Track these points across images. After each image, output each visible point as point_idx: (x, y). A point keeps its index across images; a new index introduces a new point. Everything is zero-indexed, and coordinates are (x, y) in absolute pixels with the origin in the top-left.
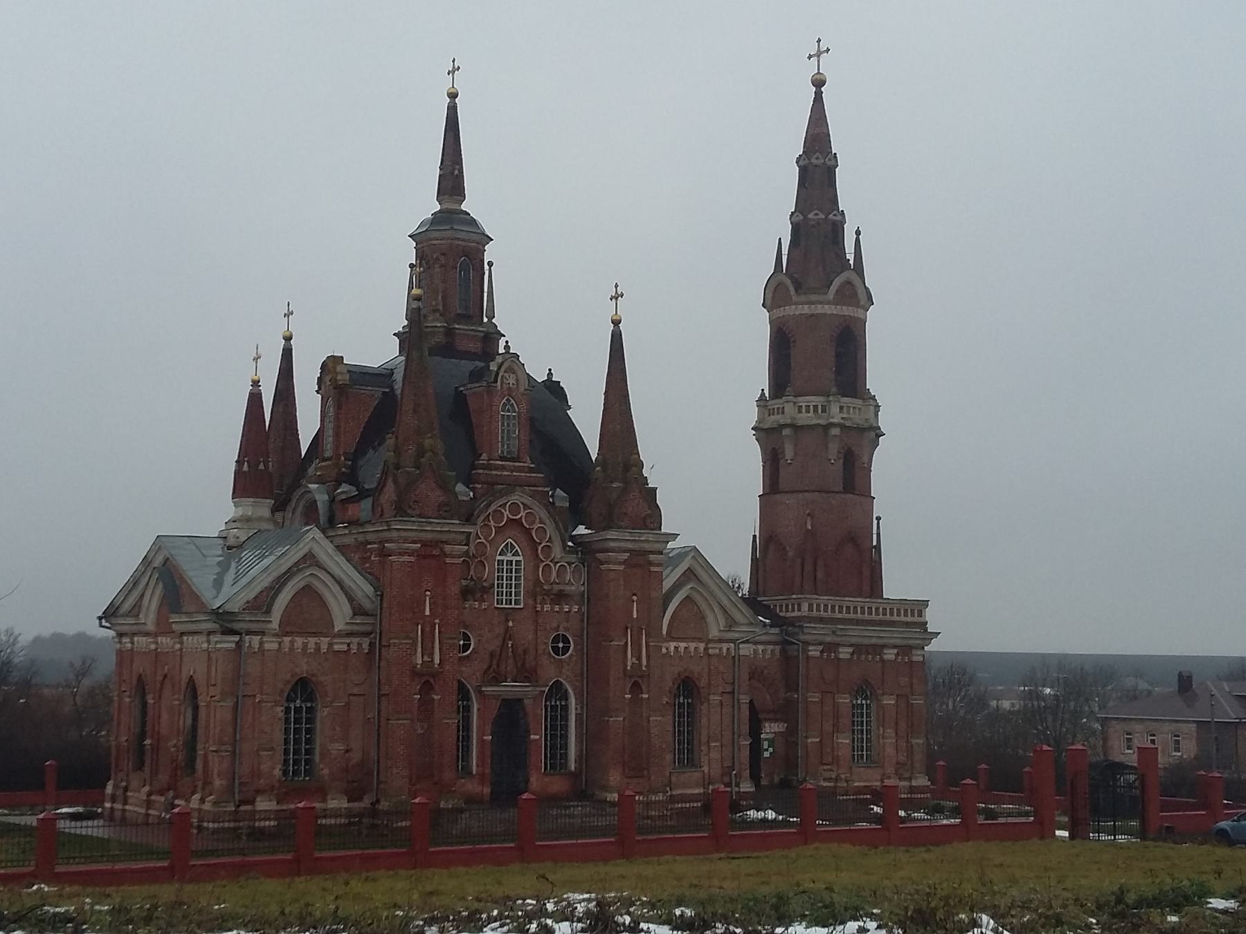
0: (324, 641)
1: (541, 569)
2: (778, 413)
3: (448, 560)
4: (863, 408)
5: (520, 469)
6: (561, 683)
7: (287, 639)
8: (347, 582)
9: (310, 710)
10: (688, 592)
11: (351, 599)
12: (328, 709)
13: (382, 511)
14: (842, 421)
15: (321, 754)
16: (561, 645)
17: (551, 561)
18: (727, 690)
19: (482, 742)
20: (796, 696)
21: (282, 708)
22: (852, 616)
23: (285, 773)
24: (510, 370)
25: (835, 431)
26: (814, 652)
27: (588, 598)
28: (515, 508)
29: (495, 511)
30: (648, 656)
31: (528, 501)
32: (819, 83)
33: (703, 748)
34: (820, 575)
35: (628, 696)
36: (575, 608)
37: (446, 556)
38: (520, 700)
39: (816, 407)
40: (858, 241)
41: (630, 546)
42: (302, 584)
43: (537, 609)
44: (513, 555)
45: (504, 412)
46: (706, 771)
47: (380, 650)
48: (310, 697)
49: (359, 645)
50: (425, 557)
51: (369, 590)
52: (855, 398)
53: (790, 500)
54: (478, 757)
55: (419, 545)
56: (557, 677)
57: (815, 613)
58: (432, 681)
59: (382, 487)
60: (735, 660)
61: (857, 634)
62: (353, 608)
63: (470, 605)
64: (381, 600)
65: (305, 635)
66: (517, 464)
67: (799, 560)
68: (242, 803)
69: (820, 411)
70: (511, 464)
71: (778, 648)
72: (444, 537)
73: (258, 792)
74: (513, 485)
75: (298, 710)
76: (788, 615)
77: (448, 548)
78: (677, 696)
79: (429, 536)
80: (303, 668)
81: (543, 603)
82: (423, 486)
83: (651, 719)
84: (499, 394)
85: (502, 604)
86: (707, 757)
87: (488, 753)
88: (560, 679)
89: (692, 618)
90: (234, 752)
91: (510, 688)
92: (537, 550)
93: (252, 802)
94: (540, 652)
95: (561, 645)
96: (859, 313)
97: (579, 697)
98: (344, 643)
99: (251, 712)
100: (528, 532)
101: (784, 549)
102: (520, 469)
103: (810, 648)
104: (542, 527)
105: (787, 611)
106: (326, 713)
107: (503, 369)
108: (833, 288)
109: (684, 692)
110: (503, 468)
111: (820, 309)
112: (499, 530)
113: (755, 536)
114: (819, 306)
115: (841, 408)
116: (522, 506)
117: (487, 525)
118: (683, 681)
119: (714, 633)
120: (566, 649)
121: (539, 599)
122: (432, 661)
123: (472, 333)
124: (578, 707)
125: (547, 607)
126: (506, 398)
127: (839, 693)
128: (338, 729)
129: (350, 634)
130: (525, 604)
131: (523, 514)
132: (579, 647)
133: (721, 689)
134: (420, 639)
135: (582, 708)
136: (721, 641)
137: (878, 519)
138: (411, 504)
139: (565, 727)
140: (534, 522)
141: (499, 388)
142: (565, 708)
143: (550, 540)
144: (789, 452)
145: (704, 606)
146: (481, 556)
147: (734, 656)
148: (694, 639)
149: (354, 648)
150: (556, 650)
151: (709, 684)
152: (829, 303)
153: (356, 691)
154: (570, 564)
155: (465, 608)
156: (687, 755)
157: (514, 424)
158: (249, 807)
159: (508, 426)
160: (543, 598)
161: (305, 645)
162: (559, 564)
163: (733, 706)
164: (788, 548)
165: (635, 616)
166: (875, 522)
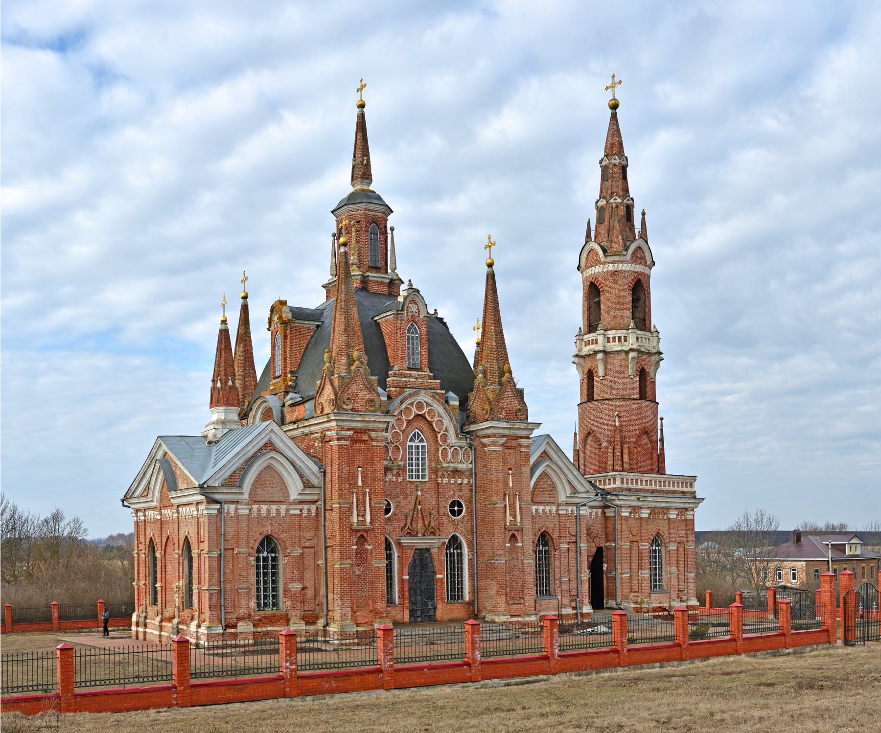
0: (283, 507)
1: (440, 452)
2: (592, 344)
3: (374, 444)
4: (651, 339)
6: (457, 536)
7: (255, 507)
8: (298, 463)
9: (274, 559)
10: (545, 469)
11: (301, 476)
12: (287, 558)
13: (323, 408)
14: (639, 347)
15: (285, 591)
16: (456, 508)
17: (447, 446)
18: (572, 541)
19: (402, 581)
20: (614, 545)
21: (253, 558)
22: (649, 487)
23: (259, 605)
24: (413, 301)
26: (625, 513)
27: (475, 473)
28: (420, 406)
29: (406, 408)
30: (521, 515)
31: (429, 400)
33: (557, 582)
34: (626, 458)
35: (508, 545)
36: (466, 481)
37: (373, 440)
38: (428, 550)
39: (620, 338)
40: (643, 220)
41: (506, 432)
43: (439, 482)
44: (419, 442)
45: (409, 333)
46: (560, 599)
47: (325, 513)
48: (273, 550)
49: (309, 510)
50: (356, 441)
51: (315, 468)
52: (645, 330)
53: (603, 406)
54: (399, 592)
55: (353, 432)
56: (454, 532)
57: (625, 486)
58: (365, 535)
59: (322, 390)
60: (578, 518)
61: (652, 501)
62: (304, 483)
63: (390, 479)
64: (325, 475)
65: (269, 503)
66: (420, 373)
67: (610, 449)
68: (228, 626)
69: (623, 341)
70: (416, 373)
71: (600, 511)
72: (371, 426)
73: (238, 619)
74: (419, 389)
75: (265, 559)
76: (606, 487)
77: (373, 435)
78: (538, 545)
79: (359, 425)
80: (268, 530)
81: (443, 476)
82: (354, 387)
83: (525, 561)
84: (405, 320)
85: (412, 478)
86: (559, 589)
87: (406, 588)
88: (457, 534)
89: (546, 488)
90: (220, 591)
91: (420, 542)
92: (437, 437)
93: (235, 627)
94: (442, 513)
95: (456, 508)
97: (470, 547)
98: (297, 509)
99: (231, 562)
100: (430, 424)
101: (599, 441)
103: (623, 510)
104: (440, 420)
105: (605, 484)
106: (286, 561)
107: (408, 301)
109: (542, 543)
110: (410, 376)
113: (575, 434)
114: (621, 265)
116: (424, 403)
117: (400, 419)
118: (542, 534)
119: (562, 498)
120: (460, 512)
121: (440, 473)
122: (365, 520)
123: (381, 280)
124: (470, 554)
126: (411, 323)
127: (642, 542)
128: (296, 572)
129: (301, 502)
130: (430, 479)
131: (426, 410)
132: (469, 510)
133: (568, 541)
134: (355, 504)
135: (473, 555)
136: (567, 504)
137: (662, 419)
138: (345, 400)
139: (461, 569)
140: (433, 417)
141: (405, 315)
142: (460, 555)
143: (446, 430)
144: (601, 372)
145: (555, 479)
146: (396, 442)
147: (576, 516)
148: (549, 503)
149: (305, 512)
150: (453, 512)
151: (560, 537)
153: (307, 544)
154: (461, 448)
155: (386, 481)
156: (544, 588)
157: (417, 343)
158: (233, 630)
159: (413, 344)
160: (443, 473)
161: (269, 511)
162: (453, 448)
163: (577, 552)
164: (602, 440)
165: (511, 485)
166: (659, 422)
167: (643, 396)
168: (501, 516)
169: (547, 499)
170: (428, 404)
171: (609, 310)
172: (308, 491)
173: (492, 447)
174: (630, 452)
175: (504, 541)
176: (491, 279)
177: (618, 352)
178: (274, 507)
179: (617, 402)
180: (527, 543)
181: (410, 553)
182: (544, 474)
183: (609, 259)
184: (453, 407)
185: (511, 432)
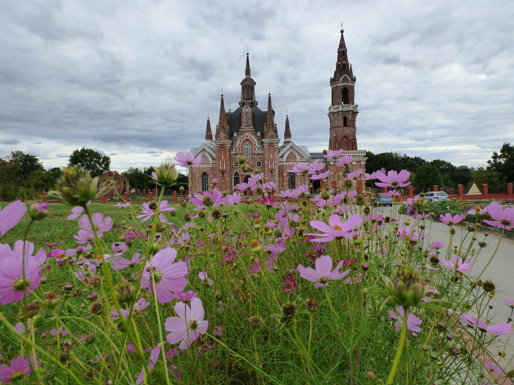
0: (208, 165)
5: (250, 129)
8: (212, 154)
9: (207, 178)
25: (340, 112)
28: (247, 136)
32: (342, 32)
41: (269, 142)
42: (202, 154)
48: (207, 176)
50: (221, 148)
72: (225, 143)
79: (222, 143)
80: (204, 171)
81: (254, 155)
96: (350, 84)
100: (251, 141)
102: (250, 129)
108: (341, 79)
111: (338, 85)
112: (244, 141)
115: (343, 107)
120: (260, 165)
125: (256, 156)
131: (249, 138)
145: (295, 154)
148: (293, 162)
149: (214, 166)
150: (258, 165)
152: (340, 83)
161: (204, 166)
167: (345, 125)
168: (267, 166)
169: (293, 160)
170: (250, 136)
171: (335, 99)
172: (213, 161)
173: (266, 146)
174: (339, 144)
175: (268, 173)
176: (270, 98)
177: (336, 112)
178: (205, 165)
179: (335, 128)
180: (276, 173)
181: (244, 176)
182: (291, 153)
183: (335, 83)
184: (259, 136)
185: (270, 142)
